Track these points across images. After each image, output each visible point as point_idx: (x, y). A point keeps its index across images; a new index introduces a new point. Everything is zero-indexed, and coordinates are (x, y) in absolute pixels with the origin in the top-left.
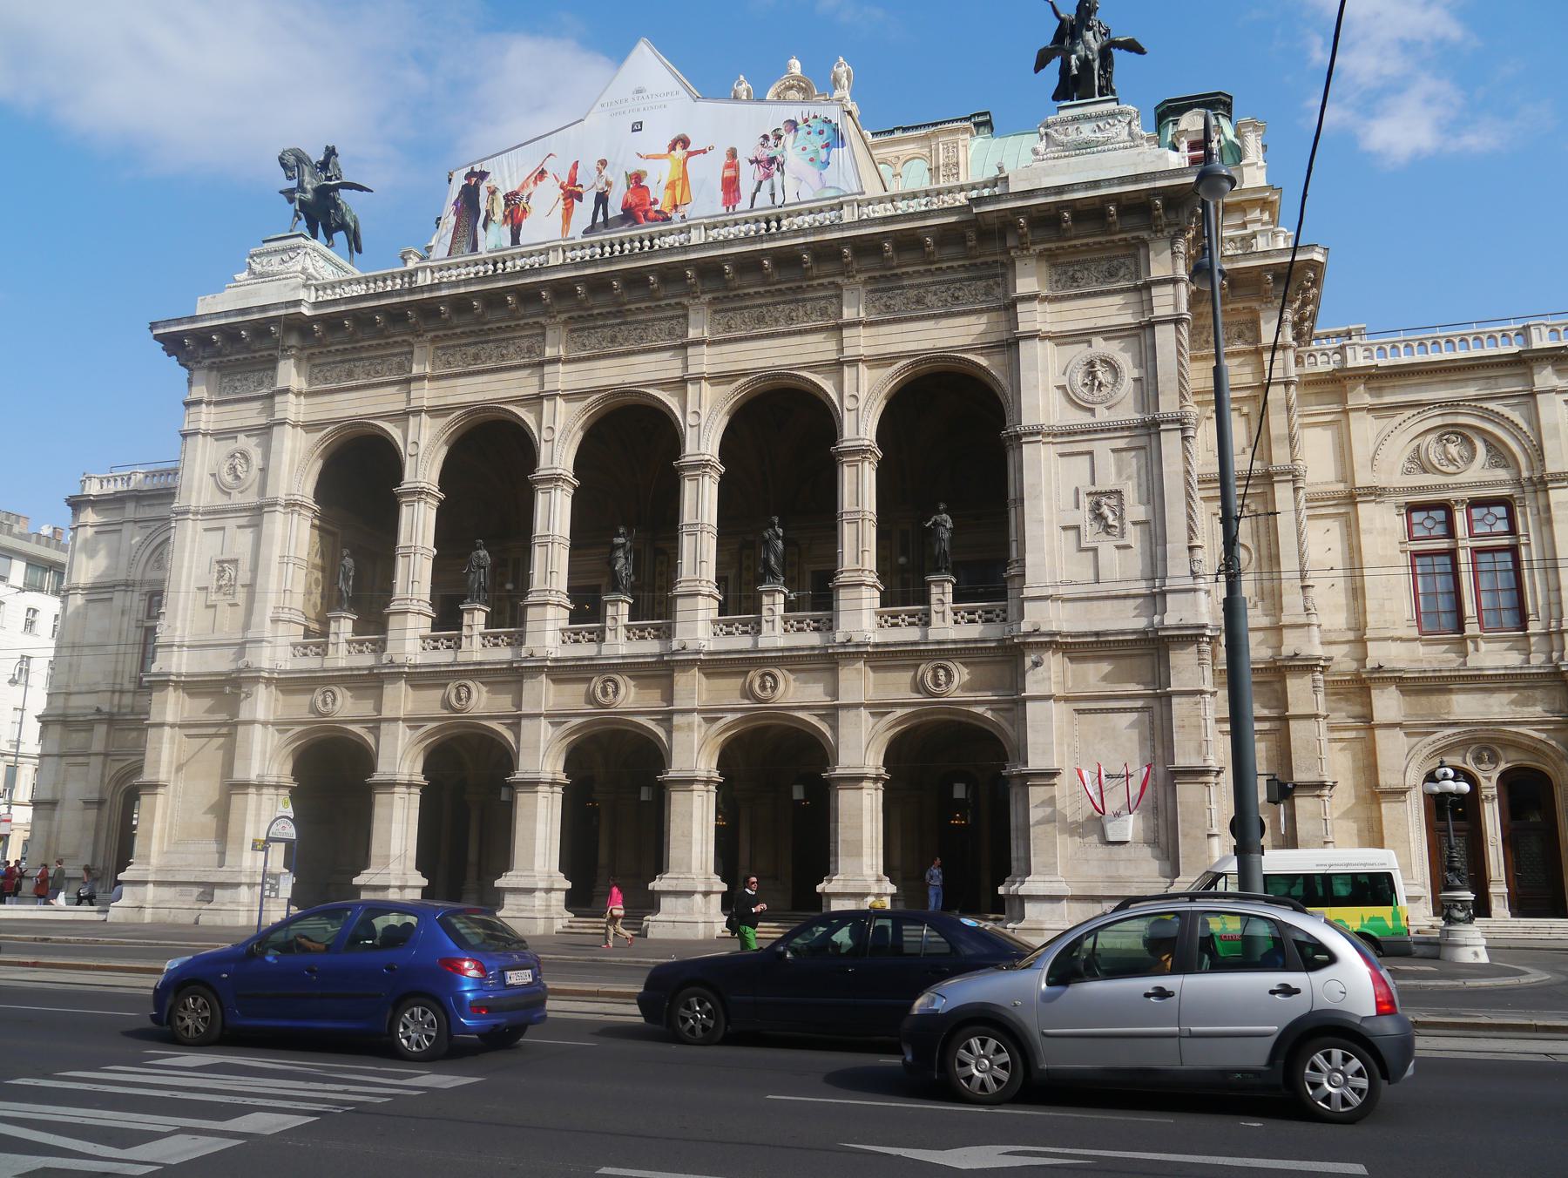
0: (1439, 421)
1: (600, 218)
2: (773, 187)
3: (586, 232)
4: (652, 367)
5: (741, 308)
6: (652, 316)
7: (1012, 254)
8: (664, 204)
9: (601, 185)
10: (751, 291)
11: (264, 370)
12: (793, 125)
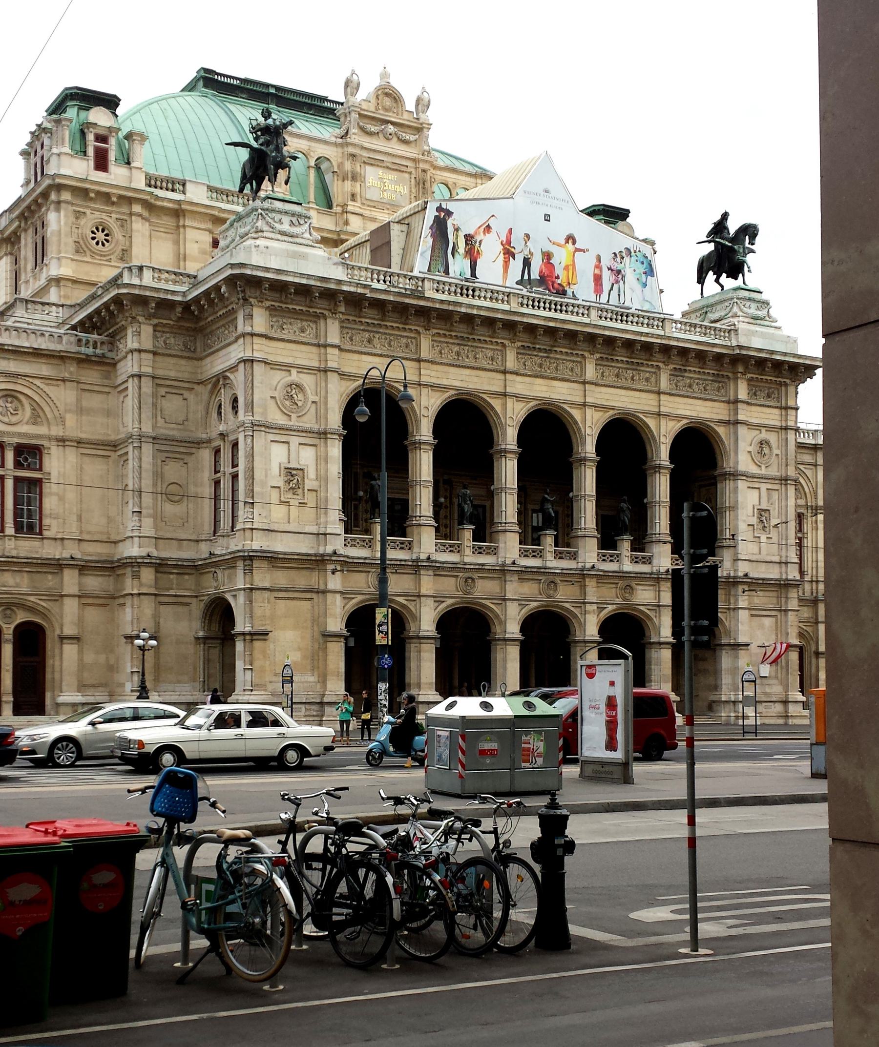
1: (526, 277)
3: (517, 283)
4: (565, 391)
5: (609, 366)
7: (739, 375)
8: (563, 280)
10: (620, 358)
11: (306, 320)
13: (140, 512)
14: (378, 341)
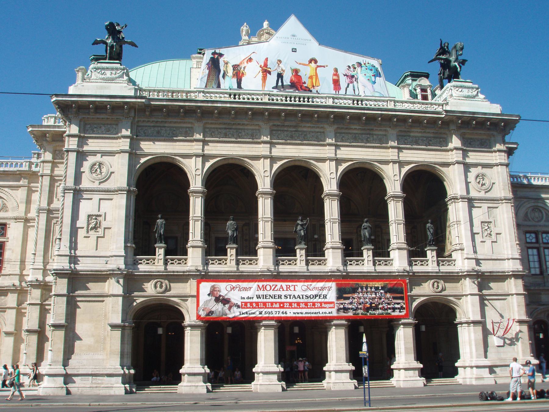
0: (533, 204)
1: (280, 84)
2: (354, 87)
3: (273, 88)
4: (311, 151)
6: (309, 130)
8: (308, 84)
9: (279, 70)
11: (111, 124)
12: (360, 64)
13: (35, 254)
14: (165, 132)
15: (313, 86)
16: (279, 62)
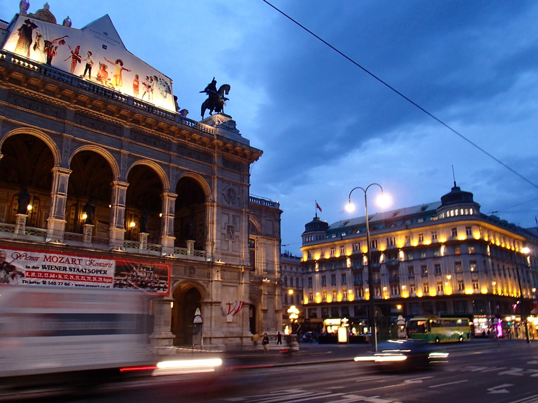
9: (89, 62)
12: (156, 78)
15: (117, 85)
16: (90, 53)
